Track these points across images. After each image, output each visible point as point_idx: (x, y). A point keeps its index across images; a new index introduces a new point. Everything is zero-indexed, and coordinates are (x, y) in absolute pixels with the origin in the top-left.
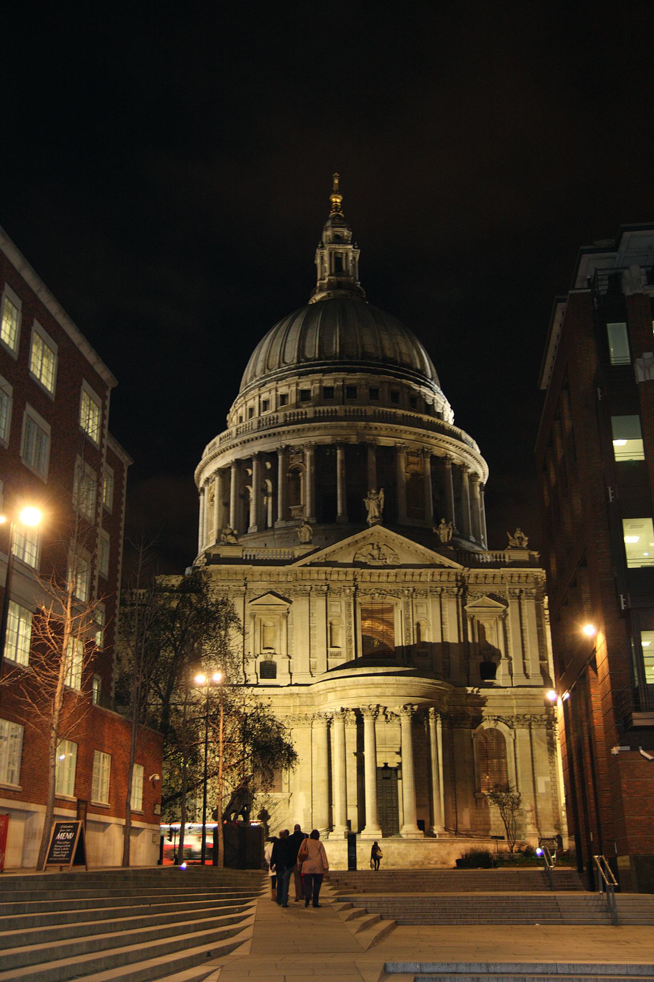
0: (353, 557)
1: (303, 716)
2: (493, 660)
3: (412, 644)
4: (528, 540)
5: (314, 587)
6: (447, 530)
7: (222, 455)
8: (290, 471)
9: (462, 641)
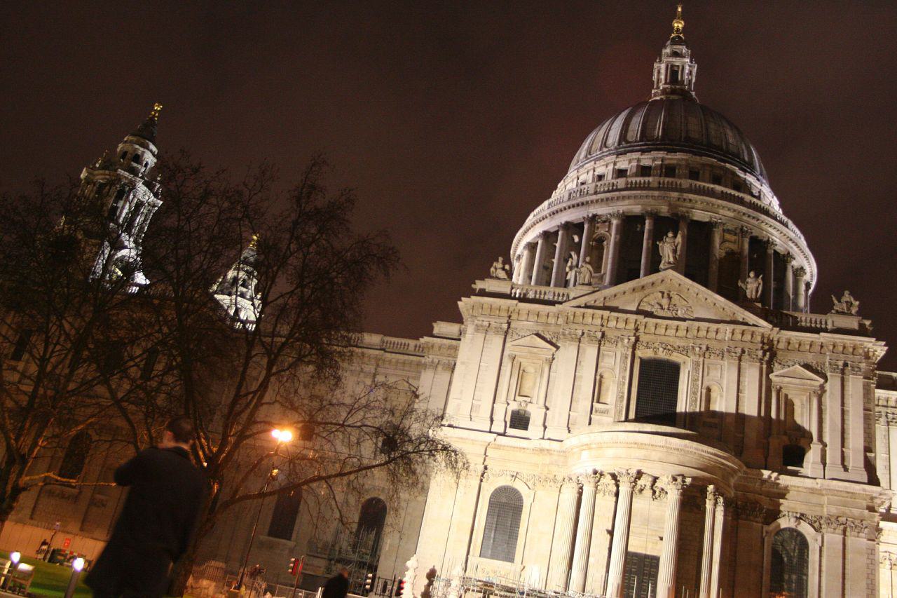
0: (637, 304)
1: (551, 477)
2: (802, 443)
3: (698, 410)
4: (859, 306)
5: (586, 331)
6: (755, 285)
7: (532, 229)
8: (594, 240)
9: (763, 414)
